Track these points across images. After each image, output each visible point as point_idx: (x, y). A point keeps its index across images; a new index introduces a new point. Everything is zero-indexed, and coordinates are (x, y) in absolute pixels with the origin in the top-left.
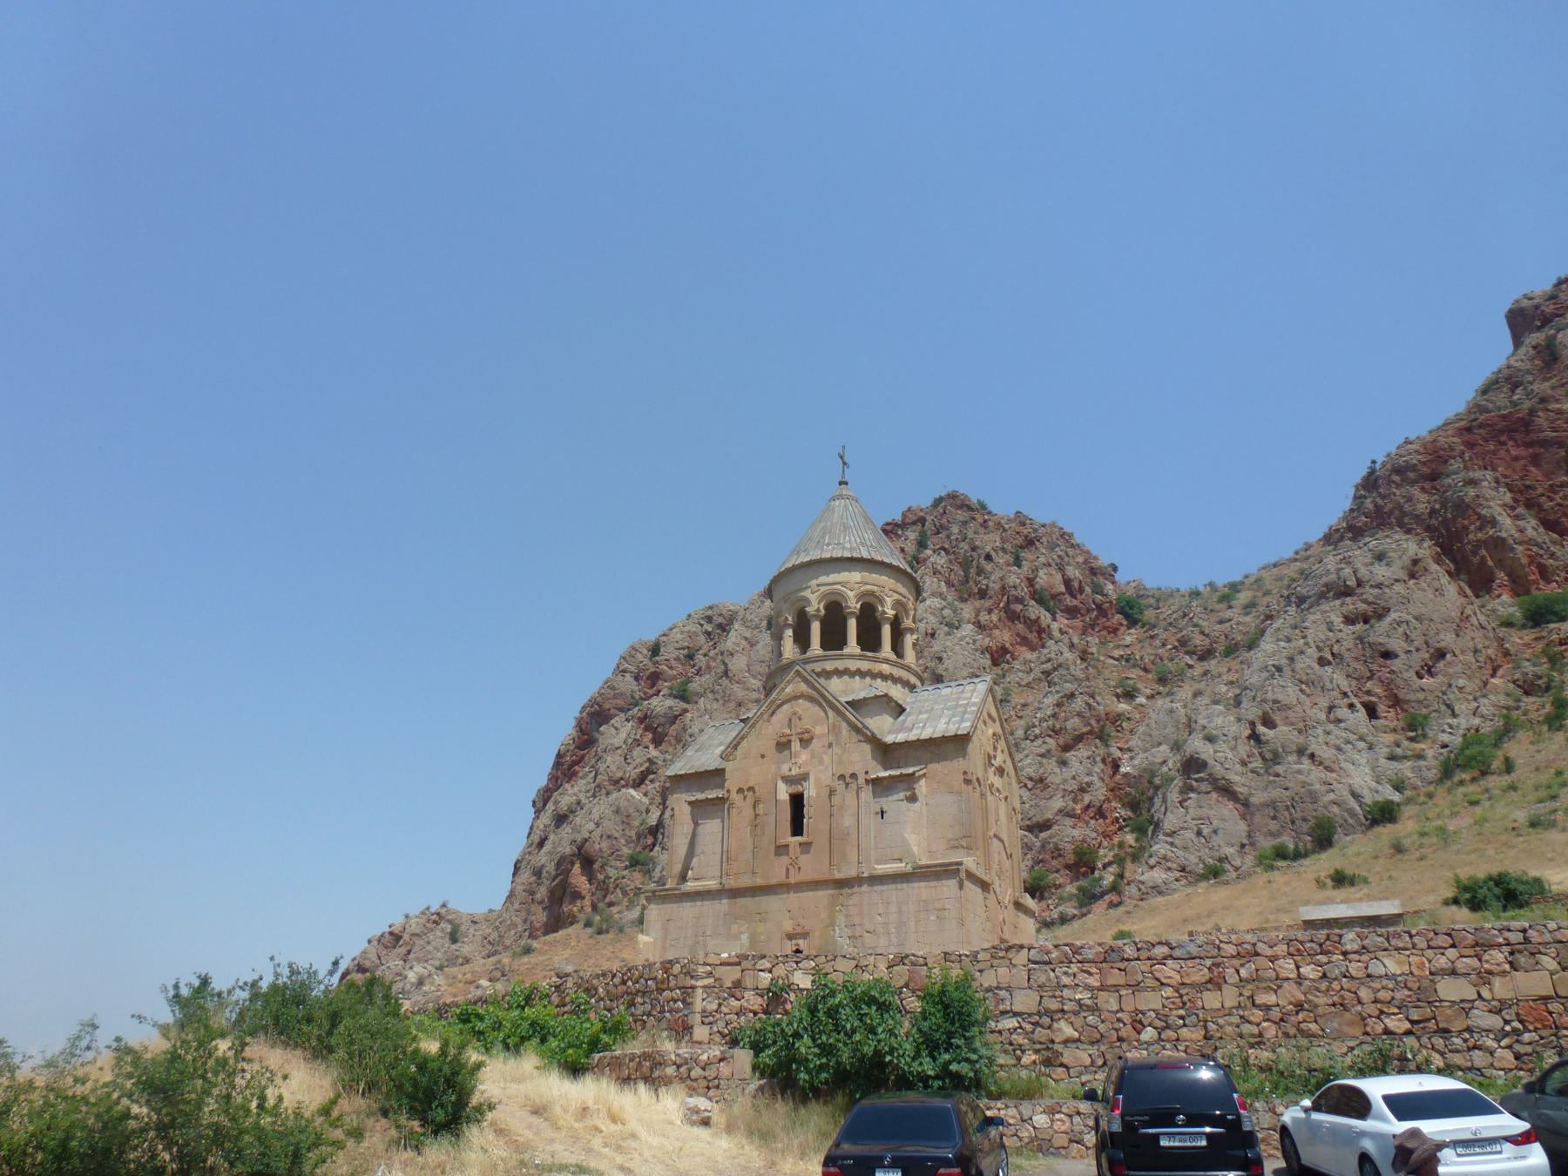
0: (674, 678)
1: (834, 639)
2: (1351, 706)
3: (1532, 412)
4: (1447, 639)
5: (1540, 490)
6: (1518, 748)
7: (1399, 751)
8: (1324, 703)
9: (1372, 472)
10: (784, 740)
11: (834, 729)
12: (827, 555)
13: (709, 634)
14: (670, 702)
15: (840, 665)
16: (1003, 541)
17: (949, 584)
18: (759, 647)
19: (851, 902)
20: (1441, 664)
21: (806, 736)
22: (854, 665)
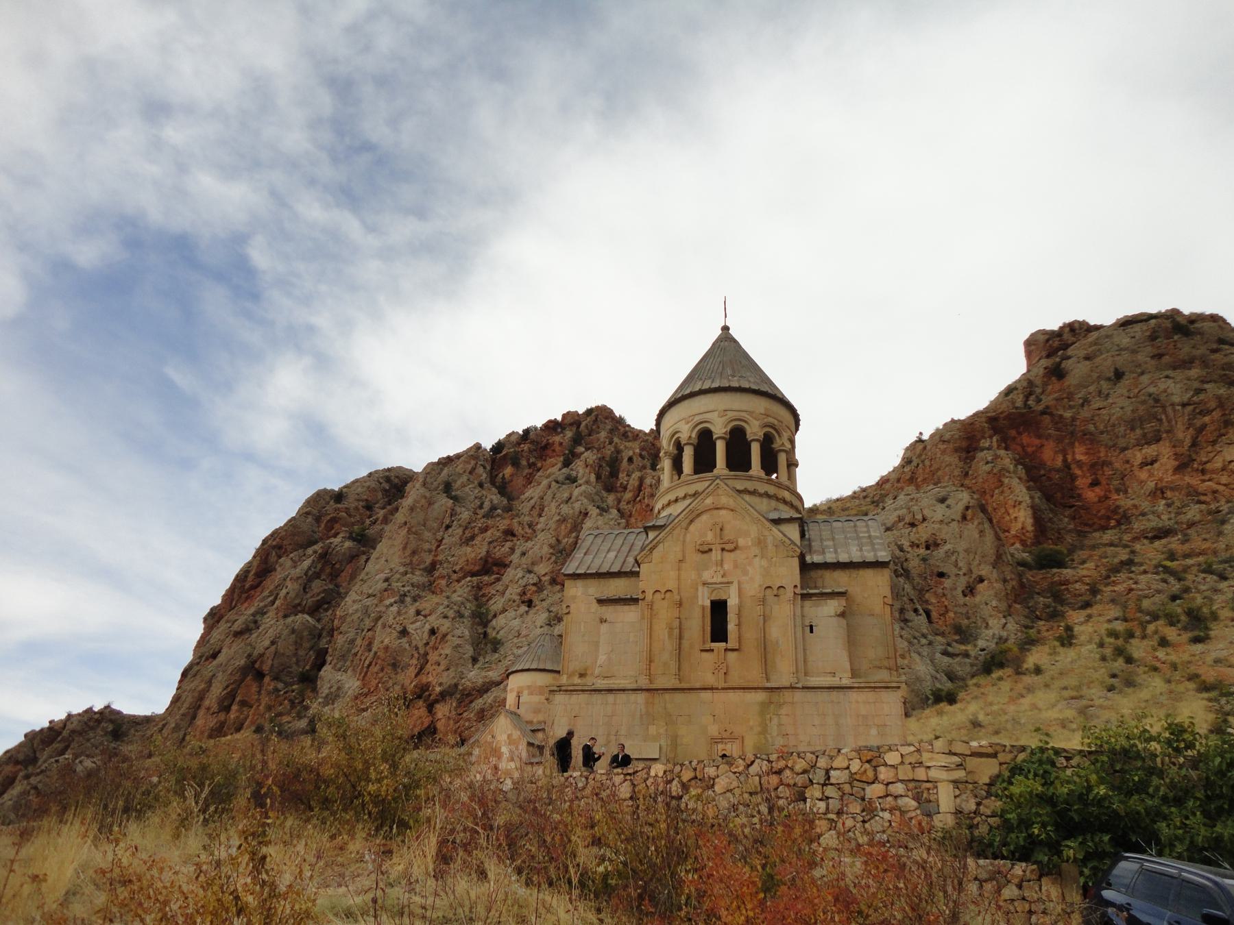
0: (353, 524)
1: (739, 461)
2: (916, 611)
3: (1043, 413)
4: (985, 570)
5: (1042, 472)
6: (1035, 657)
7: (950, 649)
8: (898, 605)
9: (920, 441)
10: (706, 548)
11: (761, 543)
12: (735, 384)
13: (386, 491)
14: (348, 544)
15: (750, 485)
16: (642, 449)
17: (598, 477)
18: (436, 506)
19: (784, 711)
20: (980, 587)
21: (731, 546)
22: (762, 488)
